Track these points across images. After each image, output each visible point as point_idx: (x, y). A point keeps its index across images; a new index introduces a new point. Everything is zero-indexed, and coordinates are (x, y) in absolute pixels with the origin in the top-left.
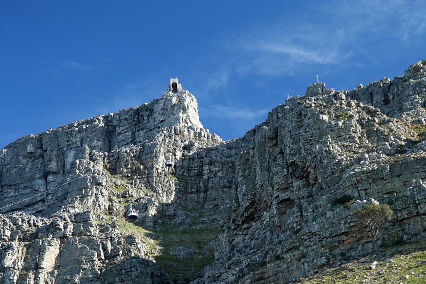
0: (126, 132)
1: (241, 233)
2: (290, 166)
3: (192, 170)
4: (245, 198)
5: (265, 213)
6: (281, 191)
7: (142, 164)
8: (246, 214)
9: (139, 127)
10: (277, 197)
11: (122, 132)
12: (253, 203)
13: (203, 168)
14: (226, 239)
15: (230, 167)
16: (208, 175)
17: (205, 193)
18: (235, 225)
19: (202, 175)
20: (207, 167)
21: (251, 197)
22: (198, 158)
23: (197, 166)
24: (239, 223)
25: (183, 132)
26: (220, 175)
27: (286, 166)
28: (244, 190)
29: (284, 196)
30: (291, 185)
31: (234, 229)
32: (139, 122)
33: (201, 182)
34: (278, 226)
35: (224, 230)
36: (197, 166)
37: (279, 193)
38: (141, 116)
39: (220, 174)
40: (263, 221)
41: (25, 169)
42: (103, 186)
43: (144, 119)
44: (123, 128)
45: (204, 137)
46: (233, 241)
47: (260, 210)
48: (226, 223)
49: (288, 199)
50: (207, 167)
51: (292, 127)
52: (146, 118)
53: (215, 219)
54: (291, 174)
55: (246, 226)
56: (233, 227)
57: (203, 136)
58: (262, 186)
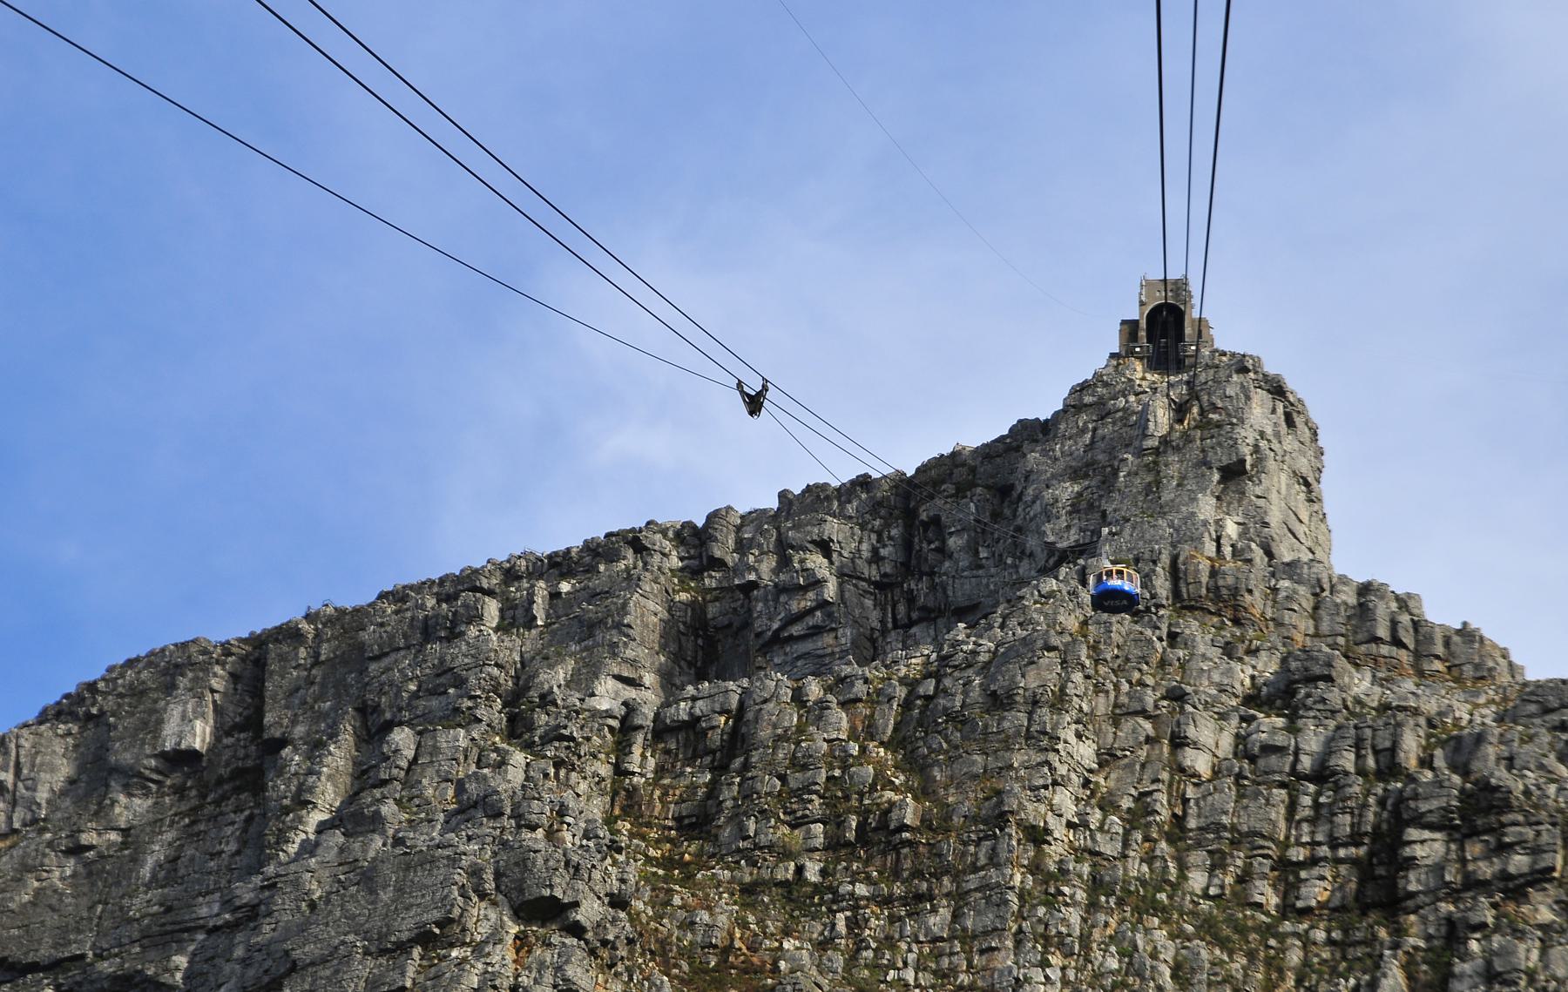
0: (817, 631)
3: (1313, 861)
7: (924, 792)
9: (911, 599)
11: (796, 630)
13: (1407, 852)
16: (1446, 907)
22: (1361, 772)
23: (1355, 839)
25: (1235, 592)
26: (1546, 915)
32: (910, 564)
36: (1355, 839)
38: (926, 525)
41: (136, 860)
42: (577, 930)
43: (943, 551)
44: (797, 605)
45: (1397, 642)
50: (1427, 847)
52: (954, 542)
57: (1383, 632)
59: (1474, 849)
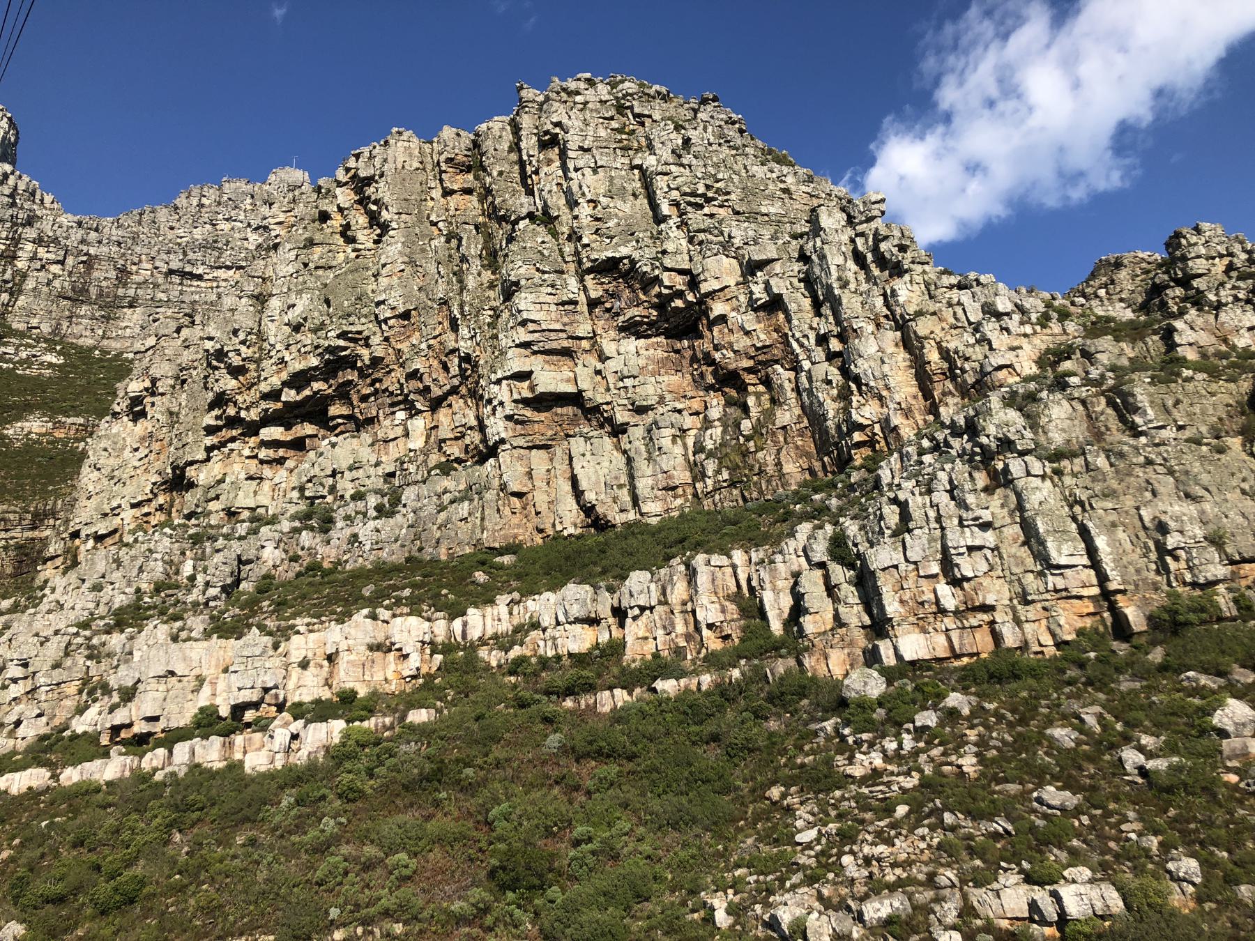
1: (247, 452)
2: (589, 271)
4: (308, 338)
5: (401, 415)
6: (540, 357)
8: (289, 395)
10: (523, 376)
12: (335, 363)
14: (143, 439)
15: (82, 262)
17: (11, 294)
18: (217, 418)
19: (14, 257)
20: (29, 247)
21: (342, 343)
23: (7, 239)
24: (243, 414)
27: (572, 267)
28: (298, 310)
29: (551, 378)
30: (585, 344)
31: (210, 430)
33: (9, 272)
34: (515, 494)
35: (143, 414)
36: (7, 239)
37: (535, 364)
39: (56, 269)
40: (386, 441)
46: (192, 463)
47: (364, 398)
48: (162, 394)
49: (576, 399)
51: (597, 138)
53: (35, 356)
54: (593, 304)
55: (274, 432)
56: (209, 419)
58: (406, 315)
59: (40, 250)
